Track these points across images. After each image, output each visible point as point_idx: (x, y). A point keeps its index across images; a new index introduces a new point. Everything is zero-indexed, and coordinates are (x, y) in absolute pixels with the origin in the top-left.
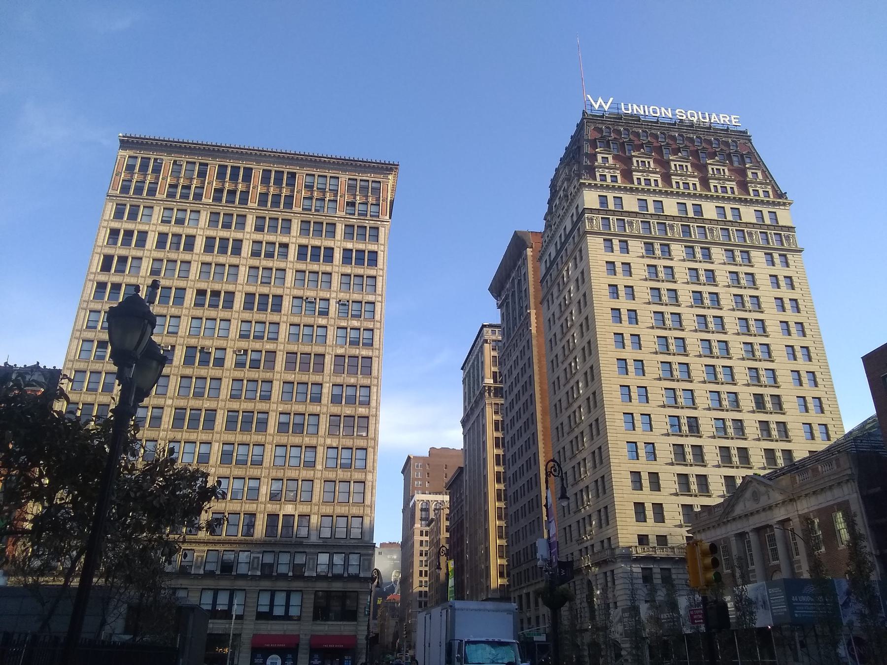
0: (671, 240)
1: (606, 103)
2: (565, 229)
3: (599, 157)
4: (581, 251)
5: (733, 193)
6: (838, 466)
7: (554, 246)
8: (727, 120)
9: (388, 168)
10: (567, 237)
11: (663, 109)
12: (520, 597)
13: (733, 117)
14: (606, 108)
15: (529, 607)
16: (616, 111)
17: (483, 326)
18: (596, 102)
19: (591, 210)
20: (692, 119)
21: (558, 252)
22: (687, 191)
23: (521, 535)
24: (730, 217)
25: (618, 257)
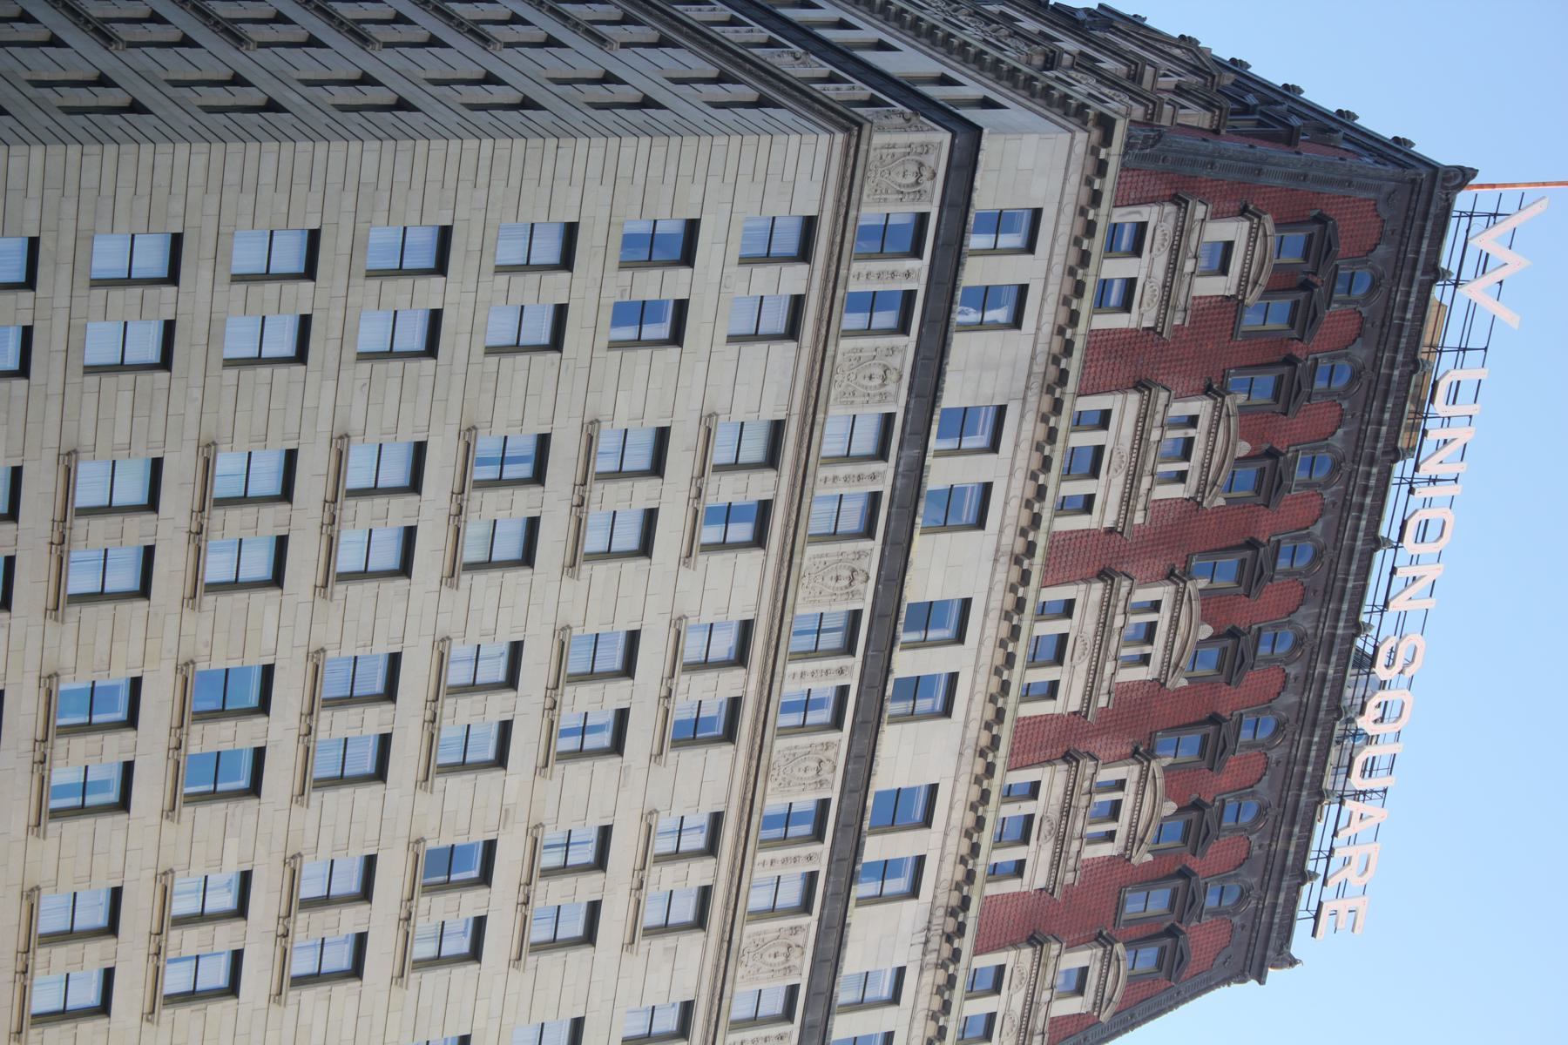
0: (788, 560)
2: (881, 46)
3: (1234, 230)
4: (761, 103)
5: (995, 873)
10: (843, 57)
16: (1452, 340)
19: (964, 167)
20: (1372, 711)
22: (1021, 650)
24: (876, 848)
25: (719, 287)
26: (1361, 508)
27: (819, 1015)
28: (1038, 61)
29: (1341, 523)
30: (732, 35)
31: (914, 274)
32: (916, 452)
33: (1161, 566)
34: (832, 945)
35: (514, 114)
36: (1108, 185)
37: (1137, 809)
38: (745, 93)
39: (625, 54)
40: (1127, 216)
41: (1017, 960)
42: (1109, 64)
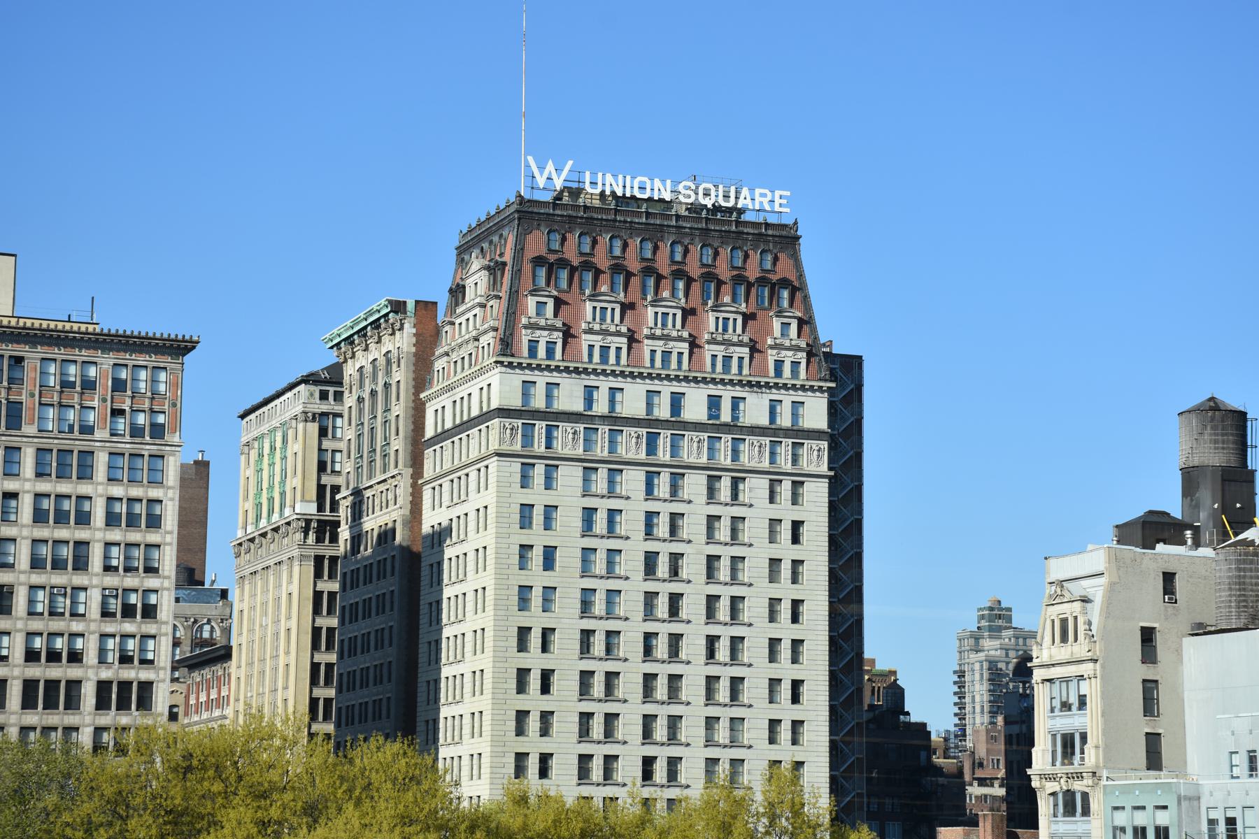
1: (558, 171)
8: (765, 200)
9: (180, 348)
13: (778, 193)
18: (542, 168)
23: (361, 578)
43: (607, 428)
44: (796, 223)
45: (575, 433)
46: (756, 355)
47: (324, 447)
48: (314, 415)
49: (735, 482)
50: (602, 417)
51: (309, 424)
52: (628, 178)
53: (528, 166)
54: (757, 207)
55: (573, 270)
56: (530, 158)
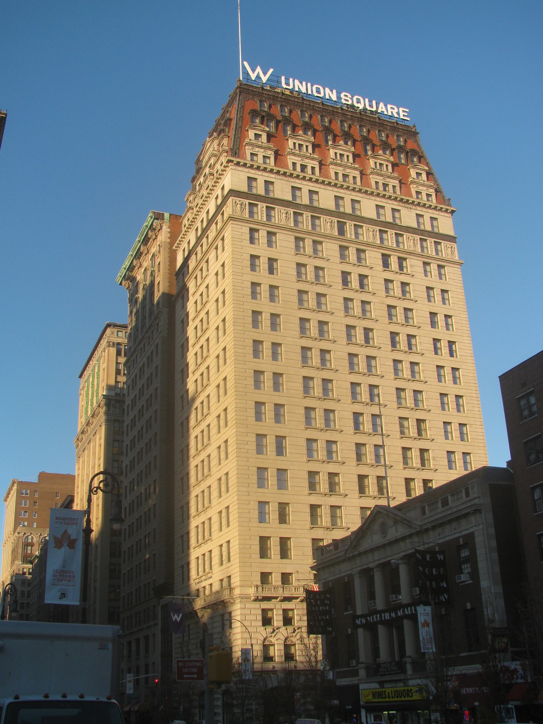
1: (265, 74)
2: (208, 212)
6: (467, 495)
7: (194, 232)
10: (210, 222)
11: (327, 90)
12: (130, 643)
13: (401, 109)
14: (264, 79)
15: (138, 653)
17: (109, 325)
20: (359, 105)
21: (199, 240)
26: (313, 106)
27: (426, 233)
28: (212, 177)
29: (317, 111)
30: (205, 248)
31: (262, 207)
32: (302, 206)
33: (327, 152)
34: (411, 230)
35: (226, 296)
36: (242, 162)
37: (381, 159)
38: (220, 244)
39: (210, 270)
40: (249, 157)
41: (413, 189)
42: (212, 161)
43: (310, 214)
44: (414, 126)
45: (287, 213)
46: (402, 186)
47: (119, 361)
48: (114, 344)
49: (401, 260)
50: (305, 206)
51: (111, 349)
52: (309, 85)
53: (244, 67)
54: (390, 114)
55: (278, 123)
56: (246, 64)
